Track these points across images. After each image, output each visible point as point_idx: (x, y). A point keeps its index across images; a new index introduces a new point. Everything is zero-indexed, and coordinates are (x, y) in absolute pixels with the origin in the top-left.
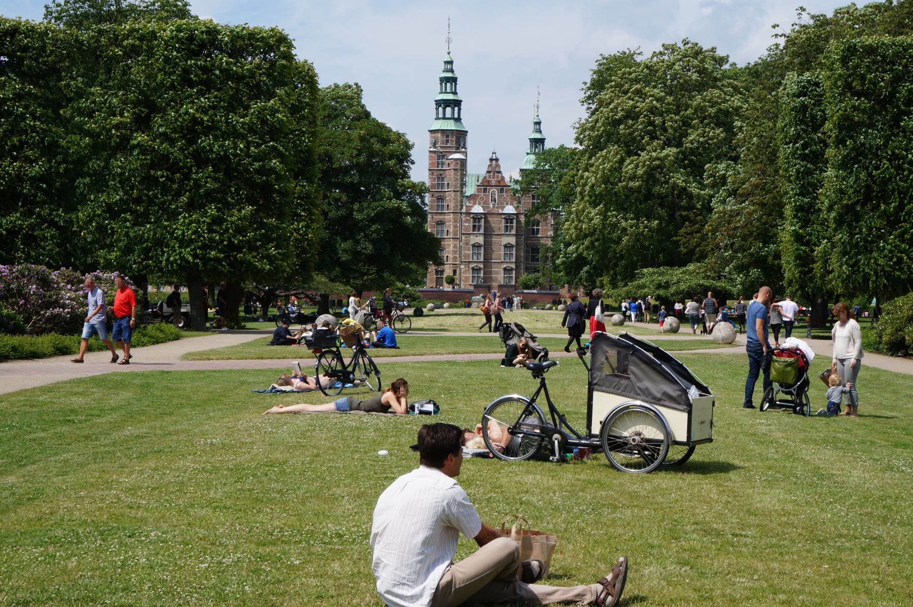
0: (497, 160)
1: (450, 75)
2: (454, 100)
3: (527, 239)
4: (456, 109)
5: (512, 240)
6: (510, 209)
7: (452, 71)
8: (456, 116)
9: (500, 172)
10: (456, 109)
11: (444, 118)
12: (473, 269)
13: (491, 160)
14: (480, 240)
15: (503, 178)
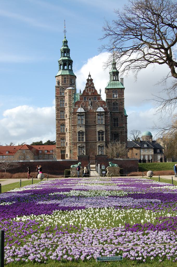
0: (91, 80)
1: (66, 48)
2: (68, 60)
3: (111, 129)
4: (70, 66)
5: (103, 129)
6: (101, 109)
7: (67, 46)
8: (70, 68)
9: (94, 87)
10: (70, 66)
11: (64, 69)
12: (79, 147)
13: (88, 80)
14: (83, 129)
15: (96, 91)
